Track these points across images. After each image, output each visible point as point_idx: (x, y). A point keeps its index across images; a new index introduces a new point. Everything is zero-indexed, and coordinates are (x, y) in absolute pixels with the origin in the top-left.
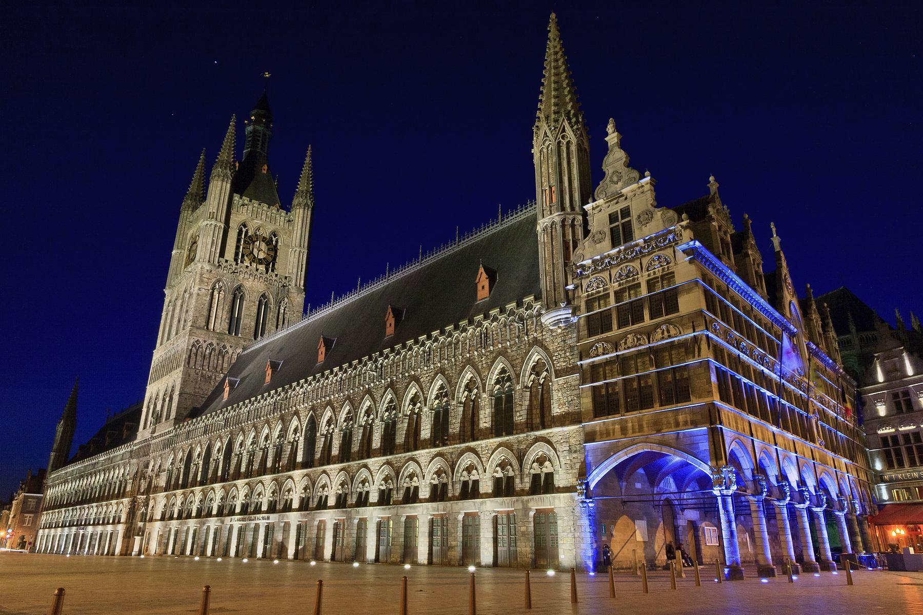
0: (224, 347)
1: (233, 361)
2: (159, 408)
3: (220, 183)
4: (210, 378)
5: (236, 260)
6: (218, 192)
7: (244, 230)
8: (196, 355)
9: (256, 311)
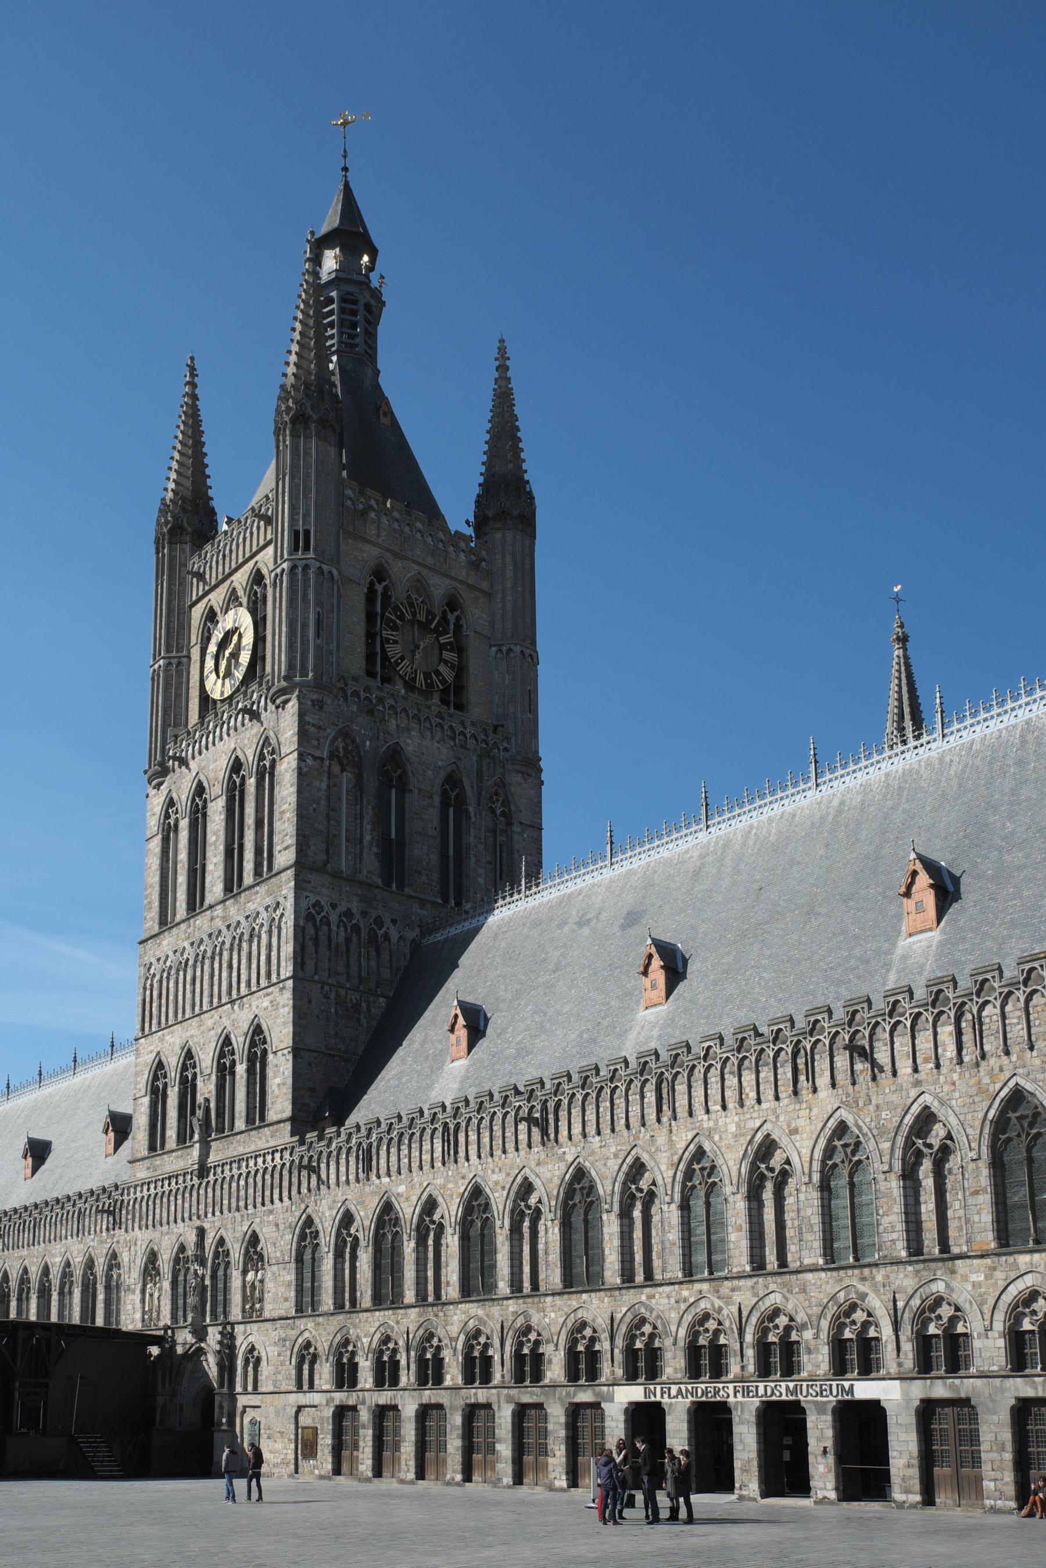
0: (379, 922)
2: (206, 1089)
4: (357, 1006)
8: (316, 942)
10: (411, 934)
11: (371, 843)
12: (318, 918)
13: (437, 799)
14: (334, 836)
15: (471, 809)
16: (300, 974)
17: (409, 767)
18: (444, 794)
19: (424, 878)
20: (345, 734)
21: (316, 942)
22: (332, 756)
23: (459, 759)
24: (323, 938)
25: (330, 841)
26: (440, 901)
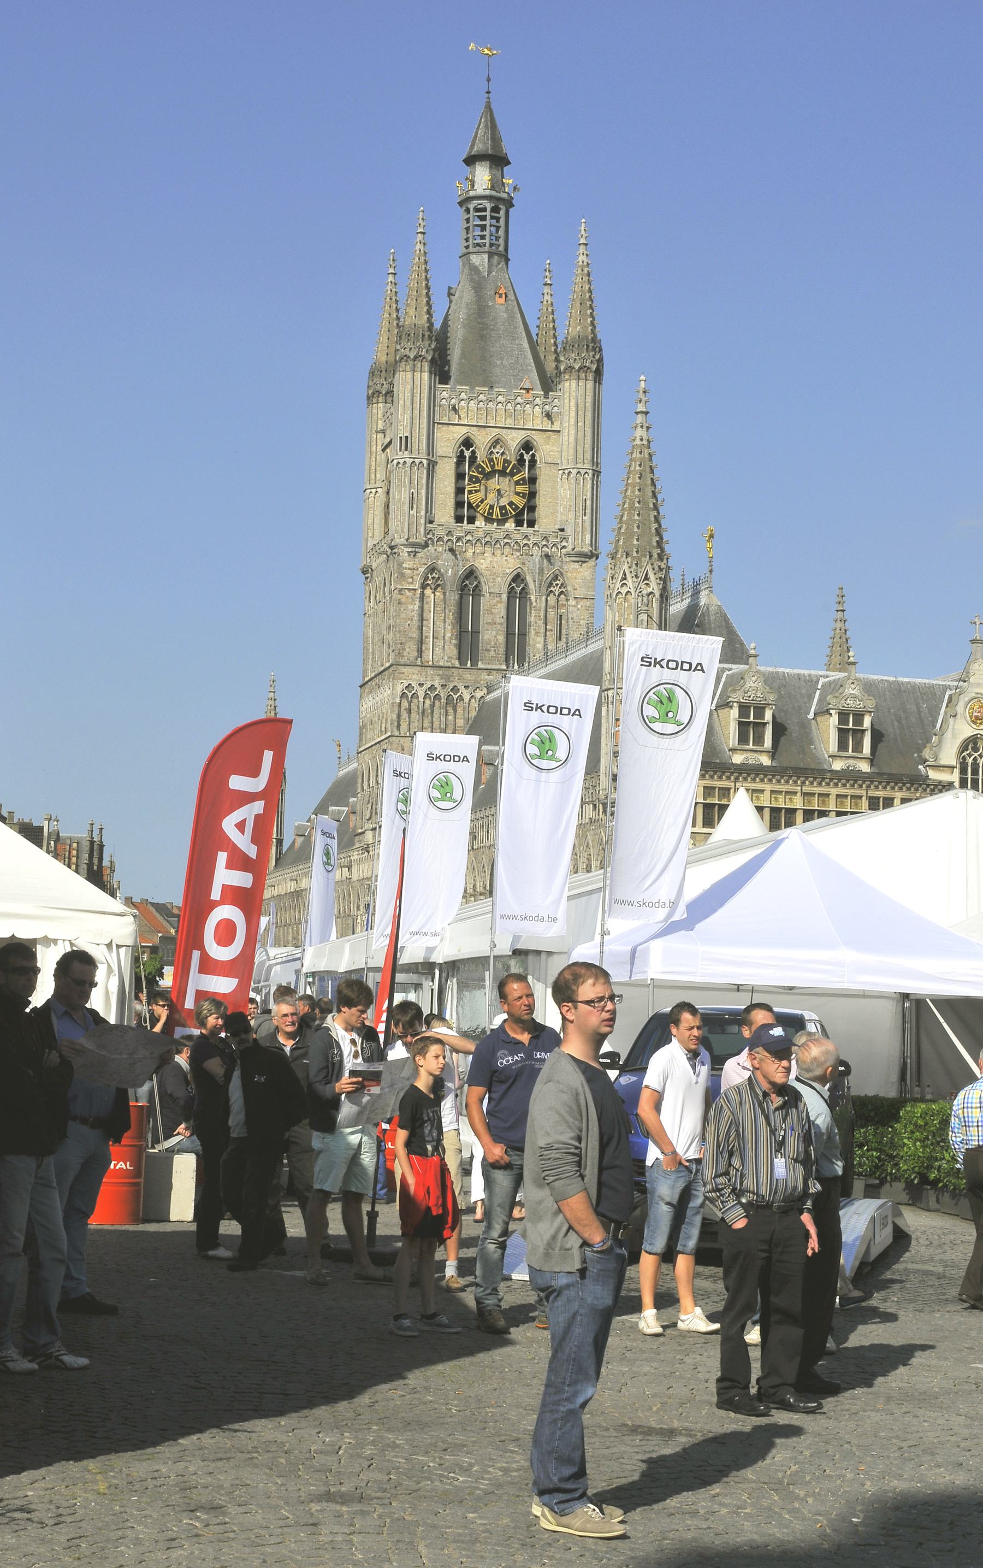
0: (455, 690)
1: (473, 714)
3: (409, 375)
5: (459, 519)
6: (408, 395)
7: (467, 454)
8: (409, 711)
9: (503, 612)
10: (479, 694)
11: (451, 638)
12: (410, 695)
13: (505, 597)
14: (426, 637)
15: (533, 598)
16: (396, 733)
17: (482, 580)
18: (511, 591)
19: (492, 653)
20: (432, 569)
21: (409, 711)
22: (424, 586)
23: (523, 564)
24: (413, 707)
25: (421, 642)
26: (504, 667)
